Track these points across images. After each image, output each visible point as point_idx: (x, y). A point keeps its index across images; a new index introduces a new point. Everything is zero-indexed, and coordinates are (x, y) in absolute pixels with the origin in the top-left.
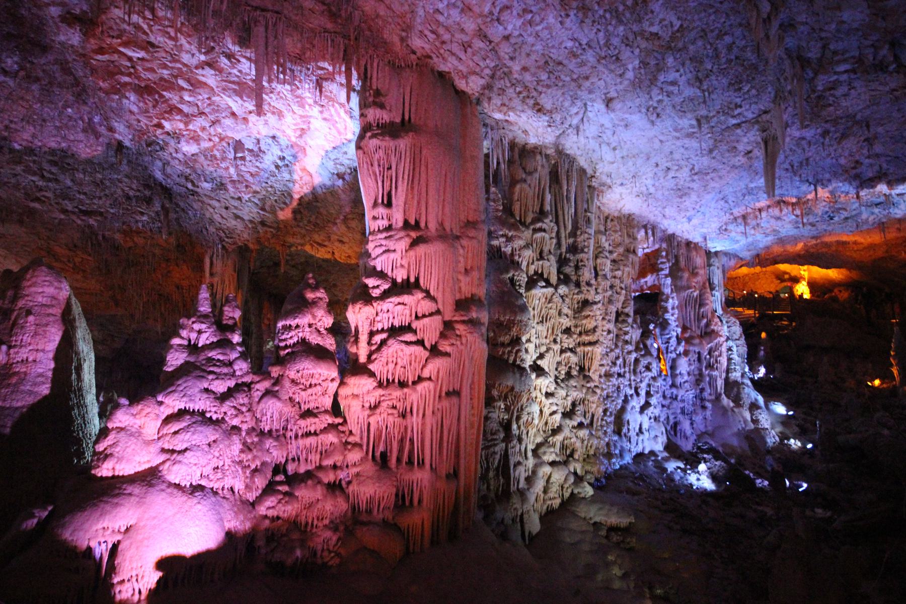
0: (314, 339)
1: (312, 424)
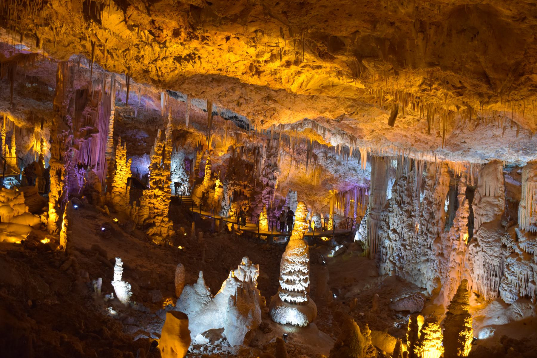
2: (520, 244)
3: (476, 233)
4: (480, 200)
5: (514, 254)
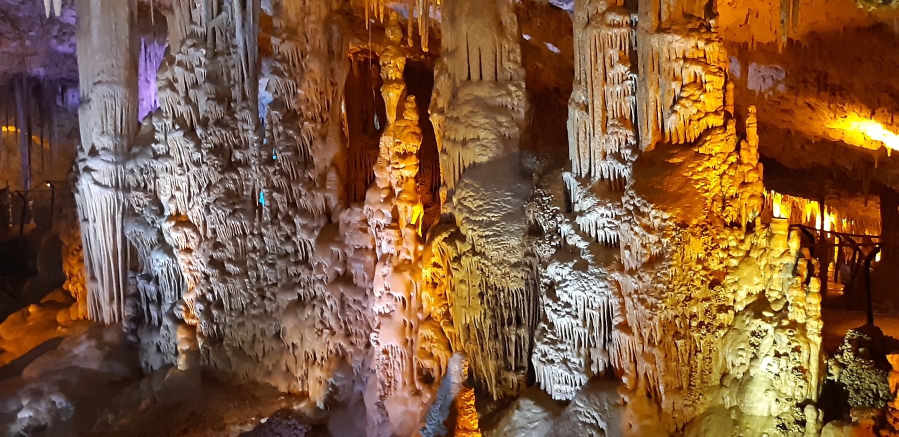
2: (579, 220)
3: (449, 199)
4: (454, 96)
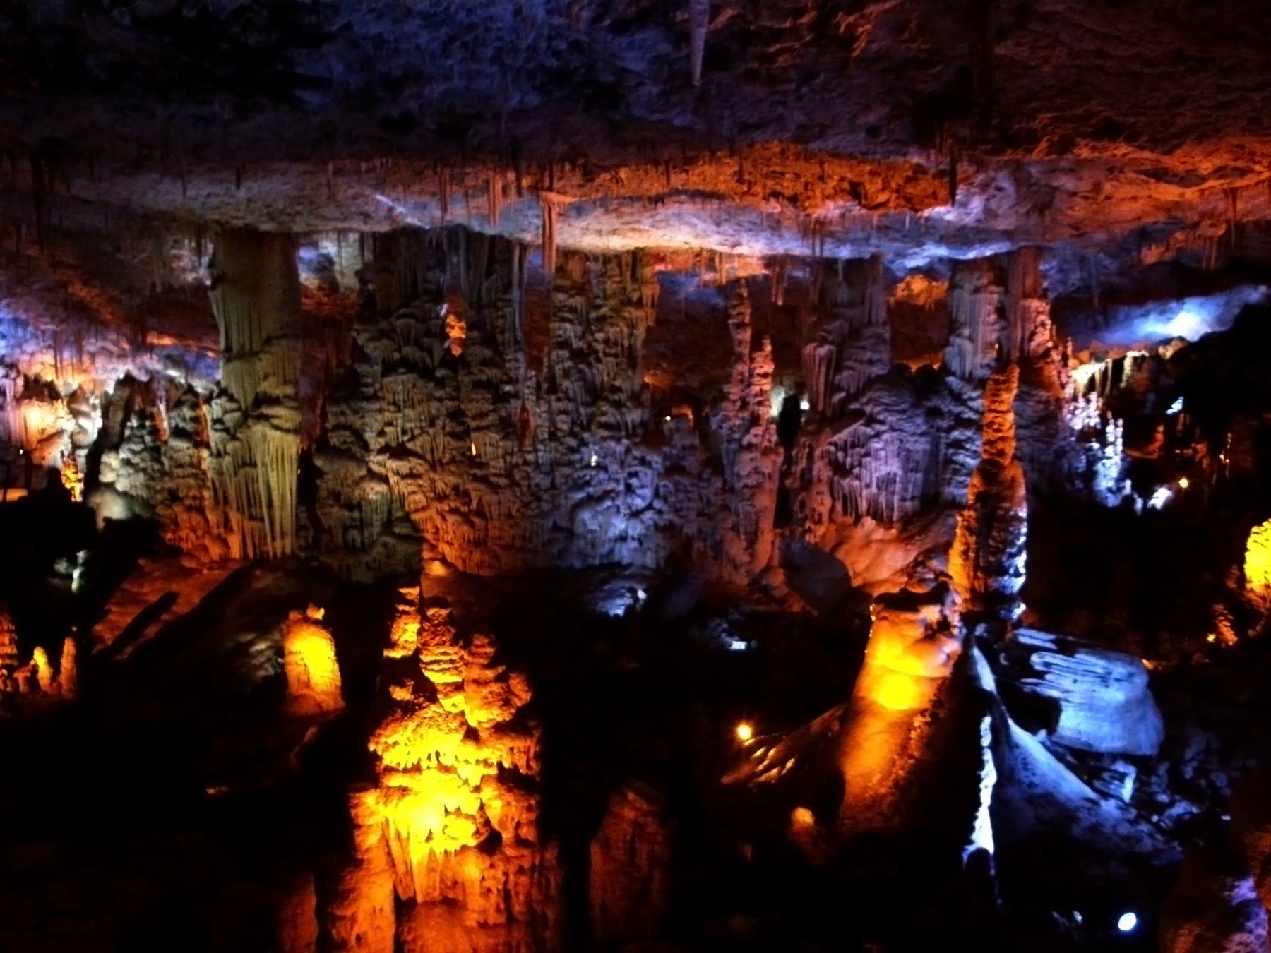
0: (182, 425)
1: (179, 471)
2: (971, 404)
5: (961, 423)
